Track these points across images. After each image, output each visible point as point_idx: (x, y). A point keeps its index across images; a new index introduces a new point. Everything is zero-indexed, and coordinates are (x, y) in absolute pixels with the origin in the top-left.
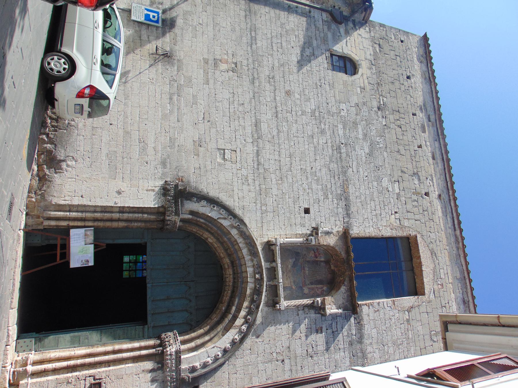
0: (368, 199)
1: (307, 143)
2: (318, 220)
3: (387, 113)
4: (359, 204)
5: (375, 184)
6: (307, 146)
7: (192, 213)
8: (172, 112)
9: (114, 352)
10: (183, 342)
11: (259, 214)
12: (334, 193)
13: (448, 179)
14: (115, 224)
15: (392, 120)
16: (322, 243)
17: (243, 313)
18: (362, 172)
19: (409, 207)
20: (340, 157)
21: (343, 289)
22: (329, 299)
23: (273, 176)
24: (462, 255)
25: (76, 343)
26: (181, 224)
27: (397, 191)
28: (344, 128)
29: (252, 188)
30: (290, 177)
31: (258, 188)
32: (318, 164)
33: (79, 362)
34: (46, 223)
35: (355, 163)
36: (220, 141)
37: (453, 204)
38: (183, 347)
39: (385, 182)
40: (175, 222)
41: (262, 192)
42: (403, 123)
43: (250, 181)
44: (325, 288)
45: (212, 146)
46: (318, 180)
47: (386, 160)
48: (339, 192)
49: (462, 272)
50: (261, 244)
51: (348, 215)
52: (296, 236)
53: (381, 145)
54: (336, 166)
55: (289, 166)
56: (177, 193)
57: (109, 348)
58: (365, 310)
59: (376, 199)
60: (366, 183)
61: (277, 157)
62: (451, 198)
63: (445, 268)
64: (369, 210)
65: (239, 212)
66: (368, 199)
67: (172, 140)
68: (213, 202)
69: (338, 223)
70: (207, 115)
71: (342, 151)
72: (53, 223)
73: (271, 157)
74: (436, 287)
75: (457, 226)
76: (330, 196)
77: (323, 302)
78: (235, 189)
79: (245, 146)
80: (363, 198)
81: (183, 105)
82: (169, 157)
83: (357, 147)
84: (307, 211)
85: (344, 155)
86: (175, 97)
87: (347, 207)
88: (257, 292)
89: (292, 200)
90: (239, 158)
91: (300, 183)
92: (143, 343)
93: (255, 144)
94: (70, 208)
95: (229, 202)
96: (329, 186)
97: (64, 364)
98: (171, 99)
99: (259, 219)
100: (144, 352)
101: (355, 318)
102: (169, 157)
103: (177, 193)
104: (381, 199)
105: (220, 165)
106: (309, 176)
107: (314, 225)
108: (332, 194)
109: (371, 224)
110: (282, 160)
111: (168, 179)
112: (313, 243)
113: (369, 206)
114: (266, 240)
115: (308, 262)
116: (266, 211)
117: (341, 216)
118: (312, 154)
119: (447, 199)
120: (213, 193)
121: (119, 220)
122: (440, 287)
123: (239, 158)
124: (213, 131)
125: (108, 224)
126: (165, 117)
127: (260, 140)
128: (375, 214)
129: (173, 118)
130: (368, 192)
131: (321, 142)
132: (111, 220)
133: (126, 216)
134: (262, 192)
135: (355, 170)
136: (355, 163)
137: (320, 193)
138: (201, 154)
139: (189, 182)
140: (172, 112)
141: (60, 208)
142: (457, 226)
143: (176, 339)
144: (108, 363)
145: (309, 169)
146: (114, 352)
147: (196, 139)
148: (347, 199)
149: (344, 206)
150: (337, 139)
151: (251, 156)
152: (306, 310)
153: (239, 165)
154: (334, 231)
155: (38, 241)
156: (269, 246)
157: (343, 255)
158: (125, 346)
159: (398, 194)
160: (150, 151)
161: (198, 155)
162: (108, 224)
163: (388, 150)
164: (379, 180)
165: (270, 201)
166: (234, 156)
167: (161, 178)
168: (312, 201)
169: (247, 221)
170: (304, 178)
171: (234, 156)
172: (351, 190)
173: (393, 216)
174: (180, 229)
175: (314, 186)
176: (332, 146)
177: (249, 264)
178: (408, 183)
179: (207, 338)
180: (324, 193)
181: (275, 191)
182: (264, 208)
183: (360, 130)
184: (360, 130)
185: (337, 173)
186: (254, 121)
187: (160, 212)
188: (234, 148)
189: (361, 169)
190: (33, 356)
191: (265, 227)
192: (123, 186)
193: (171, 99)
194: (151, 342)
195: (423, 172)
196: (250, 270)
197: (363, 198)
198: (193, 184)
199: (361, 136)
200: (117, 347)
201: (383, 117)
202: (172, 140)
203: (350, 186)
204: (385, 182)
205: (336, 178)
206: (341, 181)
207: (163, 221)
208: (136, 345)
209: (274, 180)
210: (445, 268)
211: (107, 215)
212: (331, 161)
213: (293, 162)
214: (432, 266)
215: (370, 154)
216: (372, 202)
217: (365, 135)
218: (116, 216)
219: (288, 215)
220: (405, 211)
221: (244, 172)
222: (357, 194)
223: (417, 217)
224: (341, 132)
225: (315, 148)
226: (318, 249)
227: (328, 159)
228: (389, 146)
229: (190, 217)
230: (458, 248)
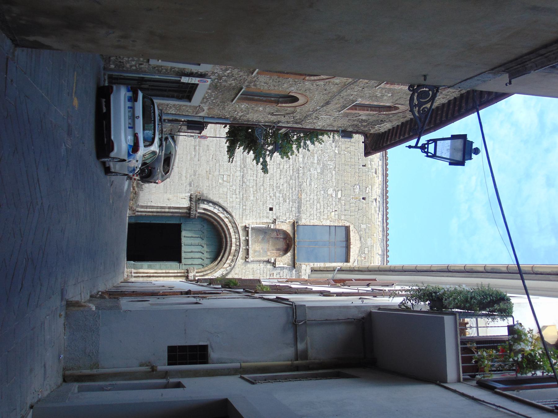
0: (315, 202)
1: (275, 168)
2: (278, 214)
3: (340, 143)
4: (308, 206)
5: (322, 192)
6: (275, 171)
7: (204, 209)
8: (195, 156)
9: (166, 273)
10: (197, 273)
11: (241, 210)
12: (291, 199)
13: (384, 188)
14: (166, 214)
15: (343, 148)
16: (278, 228)
17: (228, 261)
18: (313, 185)
19: (347, 207)
20: (298, 176)
21: (289, 254)
22: (279, 259)
23: (251, 189)
24: (385, 240)
25: (150, 267)
26: (199, 215)
27: (339, 196)
28: (303, 157)
29: (238, 196)
30: (262, 190)
31: (241, 196)
32: (282, 181)
33: (152, 275)
34: (137, 213)
35: (308, 180)
36: (221, 170)
37: (384, 206)
38: (197, 274)
39: (330, 191)
40: (195, 215)
41: (243, 200)
42: (353, 150)
43: (237, 192)
44: (281, 253)
45: (217, 173)
46: (280, 191)
47: (334, 177)
48: (294, 198)
49: (383, 251)
50: (241, 227)
51: (299, 212)
52: (263, 223)
53: (331, 167)
54: (294, 182)
55: (261, 183)
56: (197, 199)
57: (164, 271)
58: (304, 267)
59: (322, 202)
60: (316, 192)
61: (255, 178)
62: (385, 201)
63: (370, 247)
64: (315, 209)
65: (229, 210)
66: (315, 202)
67: (195, 172)
68: (215, 204)
69: (291, 217)
70: (214, 156)
71: (300, 172)
72: (139, 214)
73: (252, 178)
74: (359, 258)
75: (385, 221)
76: (288, 201)
77: (275, 260)
78: (229, 196)
79: (235, 172)
80: (311, 201)
81: (201, 151)
82: (193, 180)
83: (311, 169)
84: (271, 209)
85: (301, 175)
86: (197, 148)
87: (299, 207)
88: (237, 251)
89: (261, 203)
90: (231, 180)
91: (268, 193)
92: (179, 271)
93: (242, 171)
94: (147, 207)
95: (224, 204)
96: (287, 195)
97: (146, 275)
98: (195, 148)
99: (241, 213)
100: (179, 274)
101: (296, 271)
102: (193, 180)
103: (197, 199)
104: (326, 202)
105: (220, 184)
106: (275, 188)
107: (275, 218)
108: (289, 199)
109: (315, 217)
110: (258, 180)
111: (192, 193)
112: (272, 227)
113: (315, 207)
114: (244, 225)
115: (272, 238)
116: (245, 209)
117: (294, 212)
118: (278, 175)
119: (381, 202)
120: (215, 199)
121: (168, 212)
122: (363, 258)
123: (231, 180)
124: (218, 165)
125: (163, 214)
126: (191, 159)
127: (245, 169)
128: (319, 211)
129: (196, 159)
130: (316, 198)
131: (285, 167)
132: (165, 212)
133: (172, 210)
134: (243, 200)
135: (308, 184)
136: (308, 180)
137: (281, 199)
138: (210, 178)
139: (203, 194)
140: (195, 156)
141: (142, 207)
142: (385, 221)
143: (194, 270)
144: (164, 277)
145: (275, 184)
146: (166, 273)
147: (208, 170)
148: (300, 203)
149: (297, 206)
150: (298, 164)
151: (239, 178)
152: (265, 263)
153: (231, 184)
154: (288, 221)
155: (133, 221)
156: (246, 228)
157: (292, 235)
158: (171, 271)
159: (340, 199)
160: (184, 178)
161: (208, 179)
162: (163, 214)
163: (337, 169)
164: (325, 190)
165: (249, 203)
166: (229, 179)
167: (189, 192)
168: (275, 203)
169: (233, 214)
170: (271, 190)
171: (229, 179)
172: (304, 196)
173: (333, 213)
174: (198, 217)
175: (278, 194)
176: (293, 170)
177: (233, 237)
178: (349, 191)
179: (209, 272)
180: (284, 199)
181: (252, 198)
182: (244, 207)
183: (316, 158)
184: (316, 158)
185: (294, 186)
186: (242, 157)
187: (189, 209)
188: (229, 173)
189: (313, 183)
190: (133, 271)
191: (244, 218)
192: (170, 196)
193: (195, 148)
194: (183, 271)
195: (364, 184)
196: (234, 240)
197: (311, 201)
198: (205, 195)
199: (316, 161)
200: (167, 271)
201: (336, 147)
202: (195, 172)
203: (303, 194)
204: (330, 191)
205: (293, 189)
206: (297, 191)
207: (190, 213)
208: (176, 271)
209: (252, 192)
210: (370, 247)
211: (163, 210)
212: (291, 179)
213: (265, 180)
214: (359, 245)
215: (322, 173)
216: (318, 205)
217: (319, 160)
218: (167, 210)
219: (259, 211)
220: (343, 209)
221: (234, 187)
222: (308, 199)
223: (352, 214)
224: (301, 160)
225: (281, 171)
226: (278, 231)
227: (289, 178)
228: (337, 166)
229: (203, 211)
230: (383, 236)
